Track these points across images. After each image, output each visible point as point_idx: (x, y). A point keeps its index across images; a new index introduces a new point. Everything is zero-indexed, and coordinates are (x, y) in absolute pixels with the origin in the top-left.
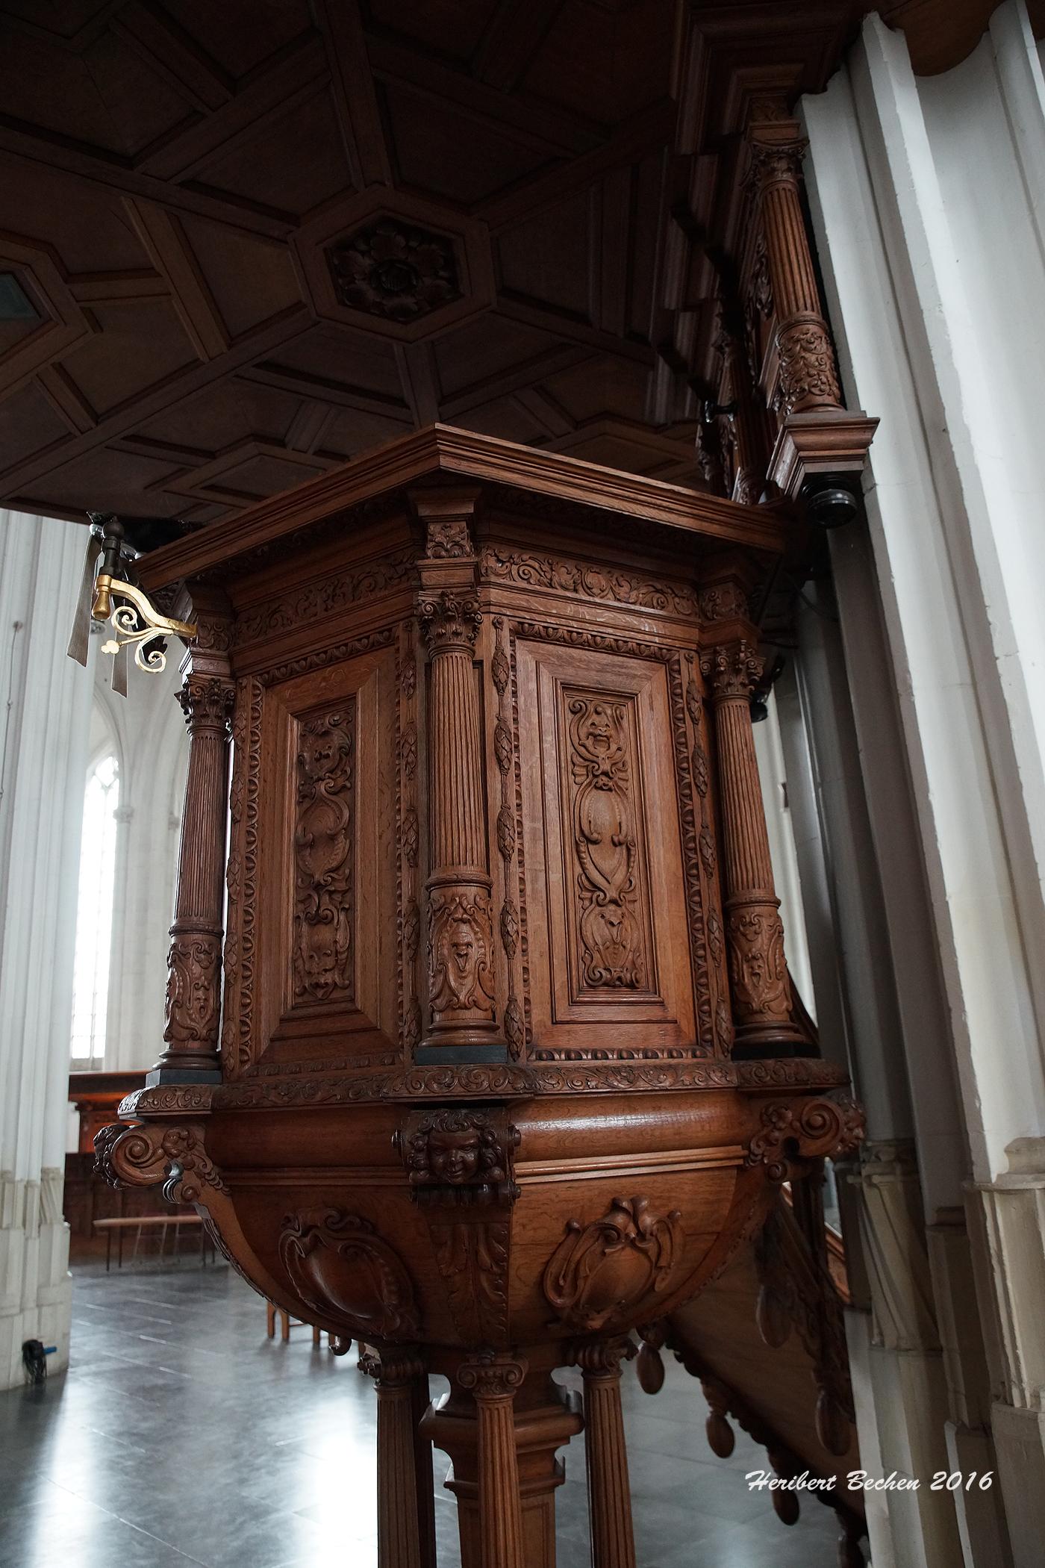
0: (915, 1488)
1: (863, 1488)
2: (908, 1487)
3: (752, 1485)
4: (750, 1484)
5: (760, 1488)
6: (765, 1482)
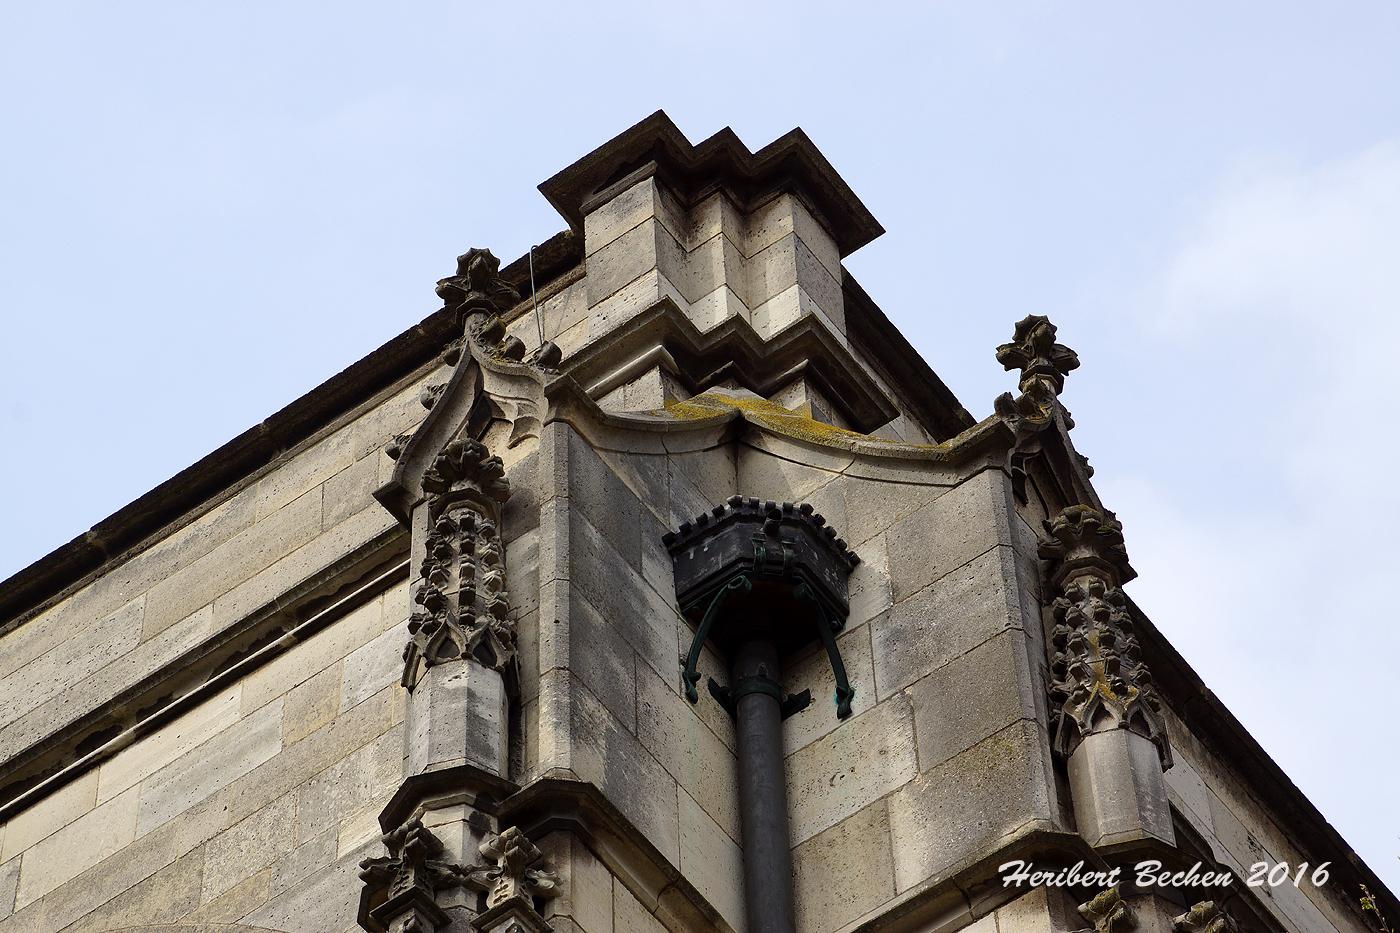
0: (1225, 884)
1: (1157, 882)
2: (1217, 882)
3: (1007, 880)
4: (1005, 879)
5: (1018, 884)
6: (1025, 876)
